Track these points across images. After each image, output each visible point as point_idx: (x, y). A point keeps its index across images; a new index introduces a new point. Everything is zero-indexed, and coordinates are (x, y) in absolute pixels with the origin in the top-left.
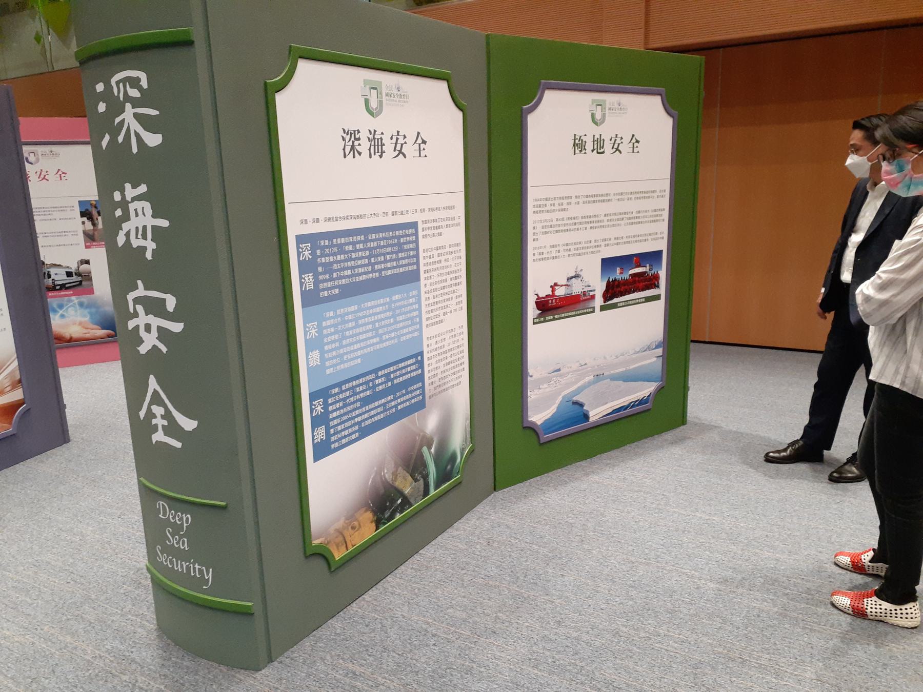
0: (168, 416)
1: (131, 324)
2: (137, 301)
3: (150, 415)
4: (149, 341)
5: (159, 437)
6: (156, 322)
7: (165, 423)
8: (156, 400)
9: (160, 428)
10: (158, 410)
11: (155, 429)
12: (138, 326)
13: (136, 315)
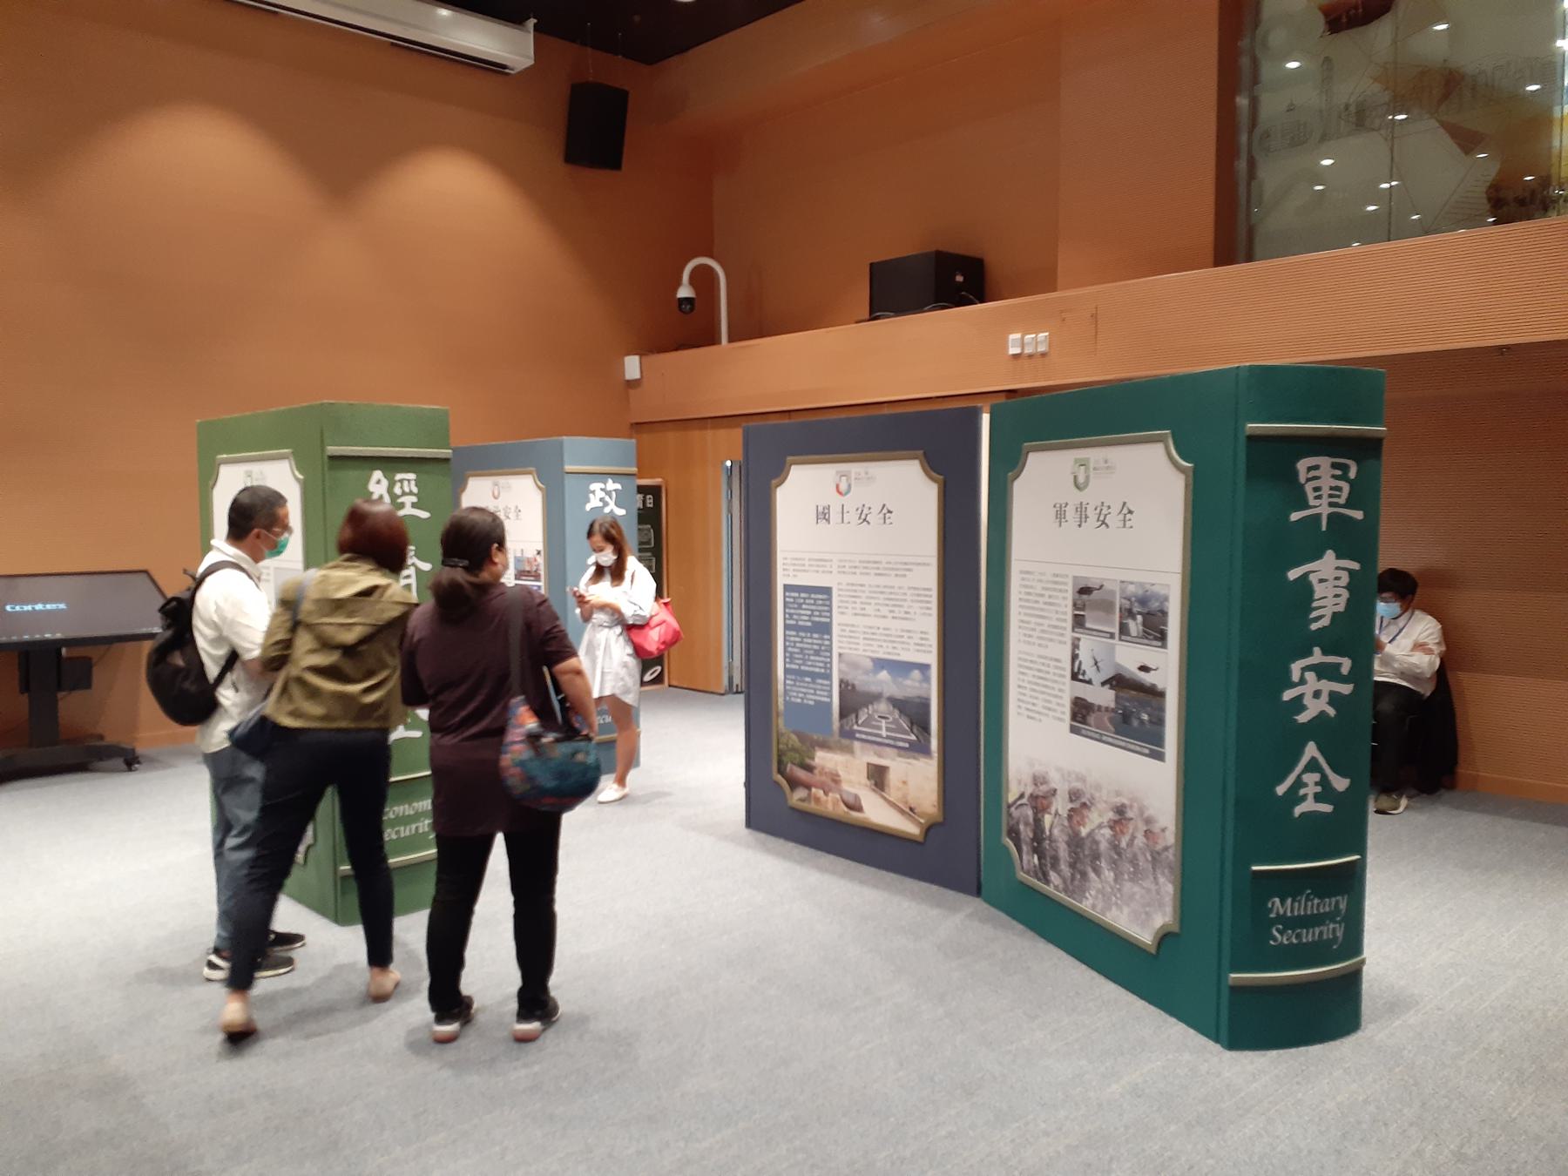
0: (1324, 782)
1: (1288, 695)
2: (1304, 670)
3: (1299, 784)
4: (1314, 708)
5: (1308, 806)
6: (1327, 686)
7: (1319, 789)
8: (1313, 766)
9: (1310, 798)
10: (1311, 778)
11: (1304, 798)
12: (1301, 696)
13: (1302, 681)
